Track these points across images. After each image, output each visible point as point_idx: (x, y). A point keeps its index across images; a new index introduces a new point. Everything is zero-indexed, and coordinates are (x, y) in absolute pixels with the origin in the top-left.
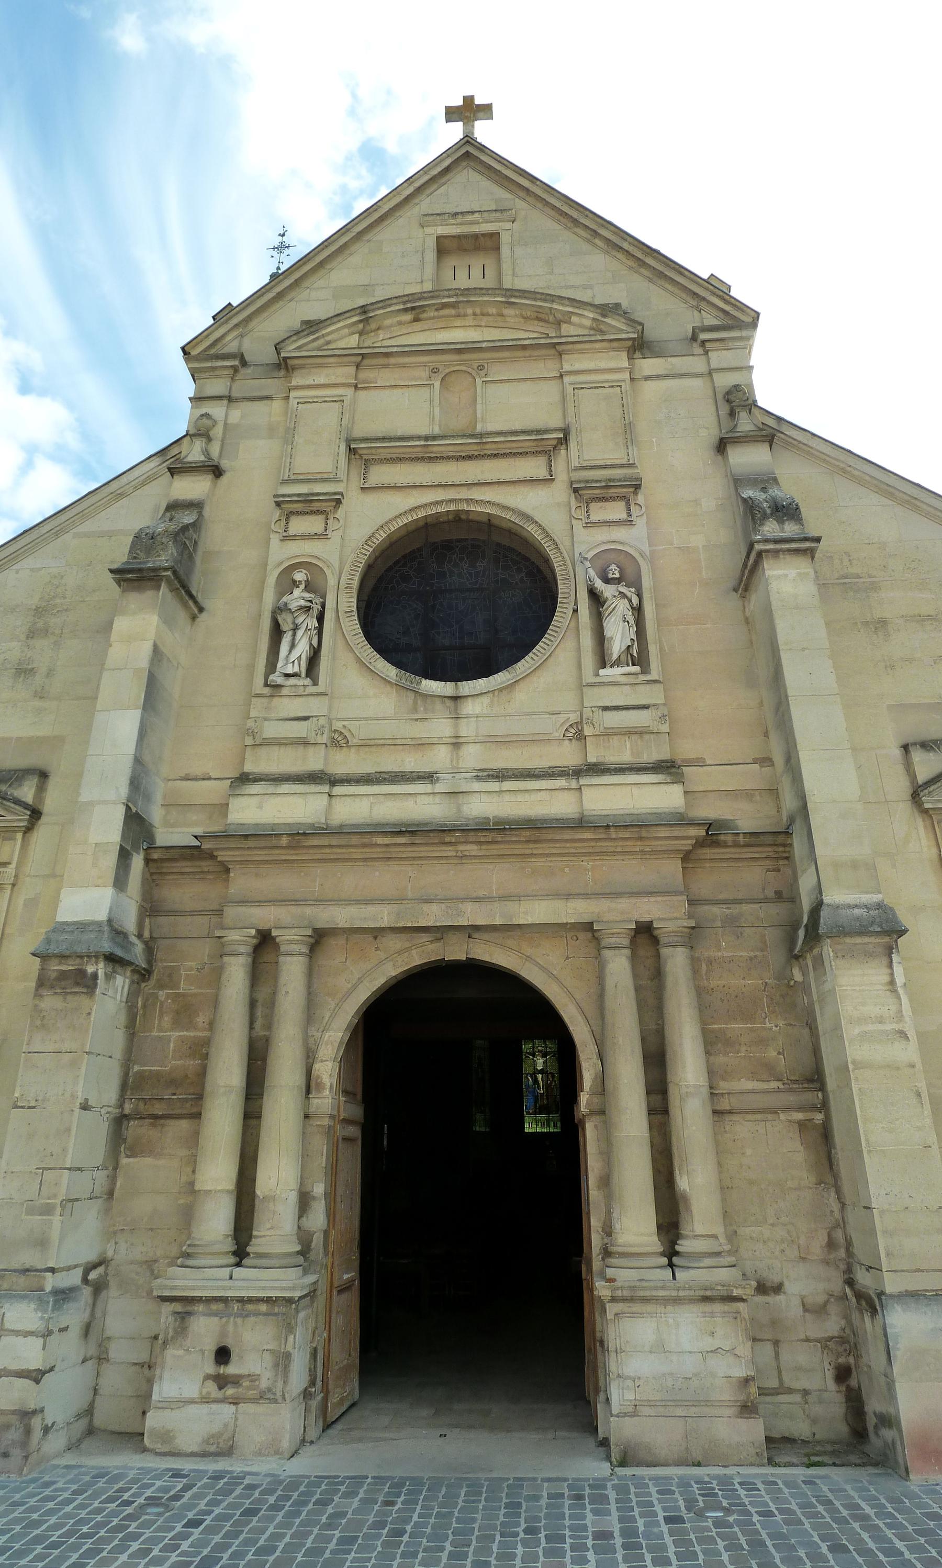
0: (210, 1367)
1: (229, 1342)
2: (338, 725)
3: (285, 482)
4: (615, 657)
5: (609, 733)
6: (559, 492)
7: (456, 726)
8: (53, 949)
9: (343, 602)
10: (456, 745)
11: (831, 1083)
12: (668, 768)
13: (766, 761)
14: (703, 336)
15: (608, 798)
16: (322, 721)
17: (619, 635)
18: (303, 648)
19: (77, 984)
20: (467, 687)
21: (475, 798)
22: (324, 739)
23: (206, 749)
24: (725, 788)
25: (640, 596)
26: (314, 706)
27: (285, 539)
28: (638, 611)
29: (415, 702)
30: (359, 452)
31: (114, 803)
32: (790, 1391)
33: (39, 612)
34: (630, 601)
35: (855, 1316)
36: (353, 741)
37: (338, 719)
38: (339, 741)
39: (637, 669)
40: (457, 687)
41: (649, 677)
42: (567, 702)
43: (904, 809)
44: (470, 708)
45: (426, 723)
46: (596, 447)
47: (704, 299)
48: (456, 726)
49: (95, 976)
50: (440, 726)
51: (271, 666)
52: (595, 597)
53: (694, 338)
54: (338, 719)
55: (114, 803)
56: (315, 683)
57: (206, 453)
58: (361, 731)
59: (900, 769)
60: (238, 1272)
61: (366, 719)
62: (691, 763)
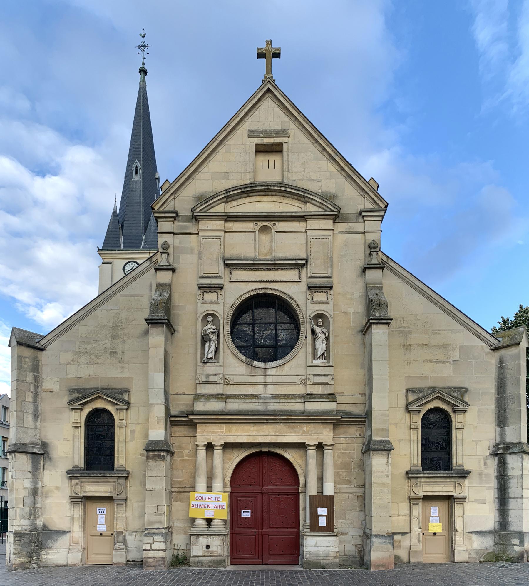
0: (205, 549)
1: (209, 544)
2: (226, 377)
3: (201, 278)
4: (319, 356)
5: (315, 384)
6: (303, 286)
7: (265, 379)
8: (150, 448)
9: (225, 328)
10: (265, 385)
11: (367, 487)
12: (332, 397)
13: (363, 395)
14: (364, 214)
15: (312, 406)
16: (221, 376)
17: (321, 348)
18: (213, 348)
19: (159, 458)
20: (269, 365)
21: (271, 404)
22: (222, 382)
23: (184, 384)
24: (349, 402)
25: (328, 332)
26: (219, 370)
27: (204, 303)
28: (327, 338)
29: (252, 369)
30: (230, 265)
31: (161, 404)
32: (347, 555)
33: (114, 328)
34: (325, 334)
35: (365, 541)
36: (232, 383)
37: (227, 375)
38: (227, 382)
39: (325, 361)
40: (265, 365)
41: (329, 364)
42: (302, 371)
43: (402, 410)
44: (269, 372)
45: (255, 377)
46: (317, 268)
47: (366, 193)
48: (265, 379)
49: (164, 456)
50: (260, 379)
51: (203, 353)
52: (313, 332)
53: (360, 213)
54: (227, 375)
55: (161, 404)
56: (218, 362)
57: (168, 261)
58: (235, 379)
59: (404, 397)
60: (209, 529)
61: (236, 375)
62: (339, 394)
